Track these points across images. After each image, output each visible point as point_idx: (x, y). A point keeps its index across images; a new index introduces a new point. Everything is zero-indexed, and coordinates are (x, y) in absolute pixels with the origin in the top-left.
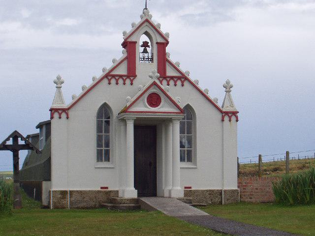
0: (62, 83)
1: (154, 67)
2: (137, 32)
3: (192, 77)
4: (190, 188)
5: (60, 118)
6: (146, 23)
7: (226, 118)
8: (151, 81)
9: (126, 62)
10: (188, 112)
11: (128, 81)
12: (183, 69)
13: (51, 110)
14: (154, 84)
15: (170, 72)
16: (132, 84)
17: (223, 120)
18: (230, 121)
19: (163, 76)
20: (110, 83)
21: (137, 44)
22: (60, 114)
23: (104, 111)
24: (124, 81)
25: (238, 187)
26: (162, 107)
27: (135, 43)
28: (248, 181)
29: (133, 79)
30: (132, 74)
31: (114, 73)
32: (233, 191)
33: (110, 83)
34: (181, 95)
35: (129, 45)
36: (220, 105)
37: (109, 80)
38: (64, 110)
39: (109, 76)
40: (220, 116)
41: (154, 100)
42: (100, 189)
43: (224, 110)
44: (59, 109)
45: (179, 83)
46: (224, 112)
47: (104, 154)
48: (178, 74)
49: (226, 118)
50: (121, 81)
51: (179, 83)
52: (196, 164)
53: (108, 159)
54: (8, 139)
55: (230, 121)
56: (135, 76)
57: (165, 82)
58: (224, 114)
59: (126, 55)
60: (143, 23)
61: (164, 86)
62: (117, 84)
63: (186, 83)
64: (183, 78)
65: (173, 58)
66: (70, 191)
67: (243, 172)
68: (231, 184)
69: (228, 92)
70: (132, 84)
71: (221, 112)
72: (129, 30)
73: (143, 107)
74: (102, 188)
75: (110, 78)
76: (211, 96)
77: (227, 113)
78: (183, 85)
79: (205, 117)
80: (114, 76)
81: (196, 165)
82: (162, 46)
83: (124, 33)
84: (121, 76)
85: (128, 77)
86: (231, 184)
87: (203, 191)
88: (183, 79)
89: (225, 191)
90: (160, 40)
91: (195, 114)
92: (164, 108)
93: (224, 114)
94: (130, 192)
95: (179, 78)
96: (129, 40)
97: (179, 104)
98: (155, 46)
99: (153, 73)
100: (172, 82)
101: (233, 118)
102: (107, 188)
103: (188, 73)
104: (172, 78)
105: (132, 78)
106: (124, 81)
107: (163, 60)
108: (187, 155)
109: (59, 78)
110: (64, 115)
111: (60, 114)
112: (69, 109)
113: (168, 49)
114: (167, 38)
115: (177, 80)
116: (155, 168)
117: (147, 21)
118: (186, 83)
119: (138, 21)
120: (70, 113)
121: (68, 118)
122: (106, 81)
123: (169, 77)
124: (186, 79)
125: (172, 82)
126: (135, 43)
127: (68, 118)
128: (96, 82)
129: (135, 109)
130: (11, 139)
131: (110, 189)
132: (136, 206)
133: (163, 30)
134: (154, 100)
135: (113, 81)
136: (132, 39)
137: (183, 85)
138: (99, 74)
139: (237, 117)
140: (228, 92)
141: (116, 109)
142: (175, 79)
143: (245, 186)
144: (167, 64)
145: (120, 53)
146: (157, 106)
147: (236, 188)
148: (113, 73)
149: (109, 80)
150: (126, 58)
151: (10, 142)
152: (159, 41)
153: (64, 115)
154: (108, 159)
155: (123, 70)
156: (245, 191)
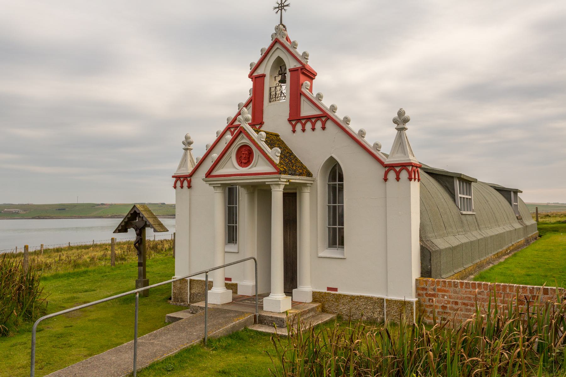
3: (339, 115)
4: (336, 290)
6: (277, 46)
7: (392, 175)
13: (173, 177)
15: (306, 110)
17: (386, 180)
18: (398, 179)
21: (267, 80)
27: (264, 76)
28: (439, 287)
32: (404, 304)
38: (185, 177)
40: (382, 171)
45: (319, 125)
48: (317, 112)
49: (392, 175)
51: (319, 125)
55: (398, 179)
57: (299, 127)
58: (387, 169)
63: (329, 124)
69: (401, 130)
71: (385, 166)
72: (256, 59)
75: (232, 130)
76: (369, 140)
77: (391, 167)
78: (324, 128)
81: (343, 254)
87: (353, 298)
88: (324, 119)
93: (387, 169)
95: (318, 118)
96: (255, 74)
100: (309, 126)
103: (333, 108)
104: (308, 119)
109: (187, 138)
114: (303, 61)
115: (316, 122)
121: (189, 187)
123: (304, 118)
124: (328, 118)
125: (309, 126)
126: (264, 76)
127: (189, 187)
128: (358, 138)
129: (219, 171)
136: (259, 72)
137: (324, 128)
140: (401, 130)
143: (434, 295)
144: (303, 98)
152: (292, 67)
153: (185, 184)
156: (432, 304)
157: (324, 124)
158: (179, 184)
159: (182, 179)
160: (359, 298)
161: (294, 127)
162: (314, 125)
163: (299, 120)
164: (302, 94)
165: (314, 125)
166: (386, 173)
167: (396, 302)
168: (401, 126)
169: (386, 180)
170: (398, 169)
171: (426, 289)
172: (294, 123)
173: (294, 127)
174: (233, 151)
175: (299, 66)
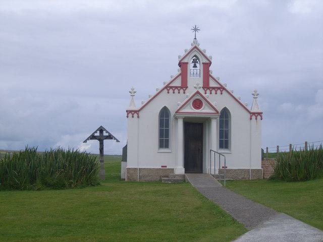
0: (135, 92)
1: (200, 81)
2: (188, 56)
5: (133, 117)
6: (195, 49)
7: (254, 117)
8: (195, 91)
9: (180, 77)
10: (225, 116)
11: (182, 91)
12: (222, 82)
14: (198, 93)
15: (212, 84)
16: (184, 93)
17: (251, 119)
19: (206, 86)
20: (168, 93)
21: (188, 65)
22: (133, 115)
23: (165, 113)
24: (179, 90)
25: (262, 167)
26: (203, 109)
27: (187, 63)
29: (186, 89)
30: (184, 86)
31: (173, 85)
32: (258, 170)
33: (168, 93)
34: (218, 101)
35: (183, 65)
36: (249, 108)
37: (168, 90)
38: (136, 112)
39: (168, 87)
40: (249, 116)
41: (197, 104)
42: (160, 167)
43: (252, 111)
44: (133, 111)
46: (252, 113)
47: (164, 142)
48: (219, 86)
49: (254, 117)
50: (176, 91)
51: (219, 92)
52: (230, 150)
53: (167, 146)
54: (96, 132)
55: (256, 119)
56: (187, 87)
57: (208, 91)
59: (180, 72)
60: (193, 49)
61: (207, 95)
62: (174, 93)
63: (224, 92)
64: (221, 88)
65: (214, 74)
66: (140, 169)
67: (265, 156)
68: (257, 164)
70: (184, 93)
72: (183, 54)
73: (190, 110)
74: (162, 167)
75: (168, 89)
77: (254, 114)
78: (221, 94)
79: (238, 118)
80: (171, 87)
82: (207, 65)
83: (179, 57)
84: (176, 87)
85: (182, 88)
86: (257, 164)
87: (235, 170)
89: (252, 170)
90: (205, 61)
91: (230, 113)
92: (205, 110)
94: (180, 169)
95: (219, 88)
97: (215, 107)
98: (202, 65)
99: (198, 85)
100: (213, 92)
101: (259, 117)
102: (166, 167)
104: (214, 88)
105: (184, 89)
106: (179, 90)
107: (207, 75)
108: (224, 143)
110: (136, 115)
111: (133, 115)
112: (139, 111)
113: (211, 68)
114: (210, 59)
116: (202, 152)
117: (195, 47)
118: (224, 92)
119: (189, 48)
120: (141, 113)
121: (138, 117)
122: (166, 91)
124: (224, 89)
126: (187, 63)
127: (138, 117)
130: (98, 132)
131: (167, 168)
132: (183, 180)
133: (208, 54)
134: (197, 104)
135: (171, 91)
136: (185, 61)
137: (221, 94)
138: (162, 86)
139: (261, 117)
141: (172, 111)
142: (216, 89)
144: (210, 78)
145: (176, 71)
146: (199, 109)
147: (260, 168)
148: (171, 85)
149: (168, 90)
150: (180, 74)
151: (98, 134)
154: (167, 146)
155: (178, 83)
157: (221, 91)
158: (130, 115)
159: (133, 113)
160: (239, 170)
161: (206, 91)
162: (216, 91)
163: (209, 88)
164: (210, 75)
165: (216, 91)
166: (251, 117)
167: (255, 170)
168: (255, 97)
169: (251, 119)
170: (256, 115)
171: (265, 164)
172: (206, 89)
173: (206, 91)
174: (191, 102)
175: (207, 62)
